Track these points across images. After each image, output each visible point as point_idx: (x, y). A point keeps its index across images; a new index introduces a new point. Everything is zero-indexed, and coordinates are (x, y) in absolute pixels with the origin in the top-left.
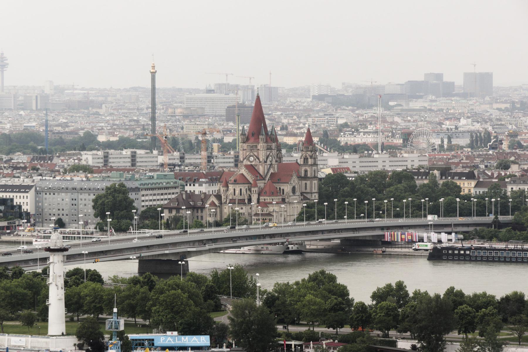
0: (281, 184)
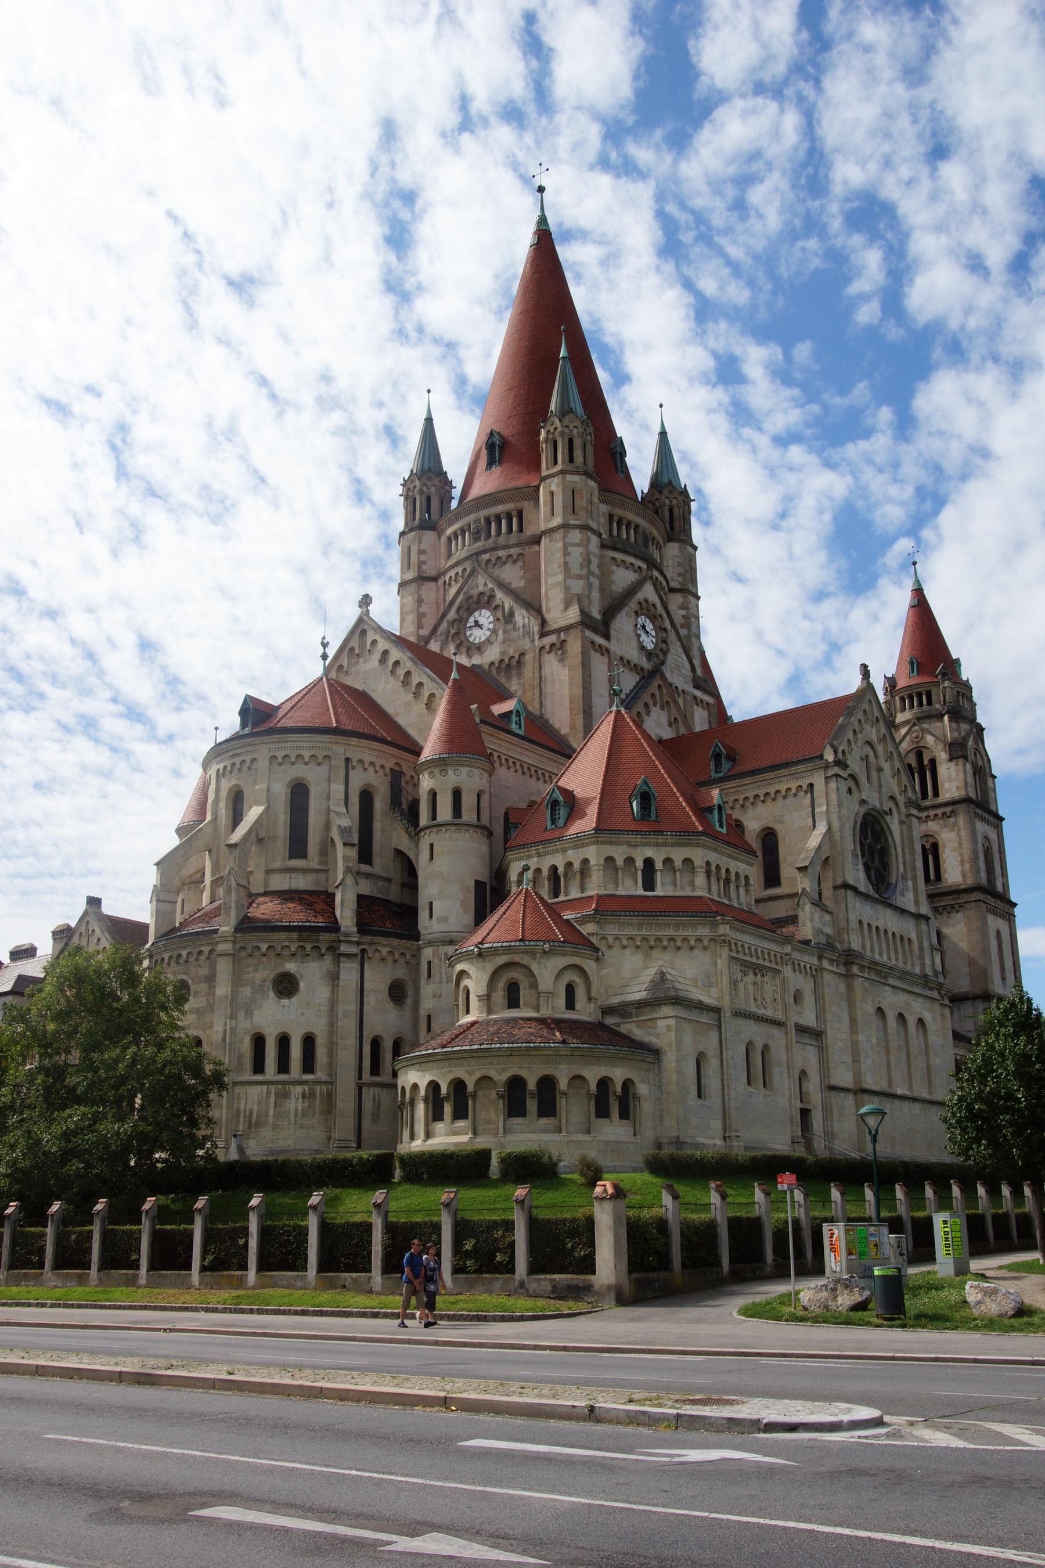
0: (750, 789)
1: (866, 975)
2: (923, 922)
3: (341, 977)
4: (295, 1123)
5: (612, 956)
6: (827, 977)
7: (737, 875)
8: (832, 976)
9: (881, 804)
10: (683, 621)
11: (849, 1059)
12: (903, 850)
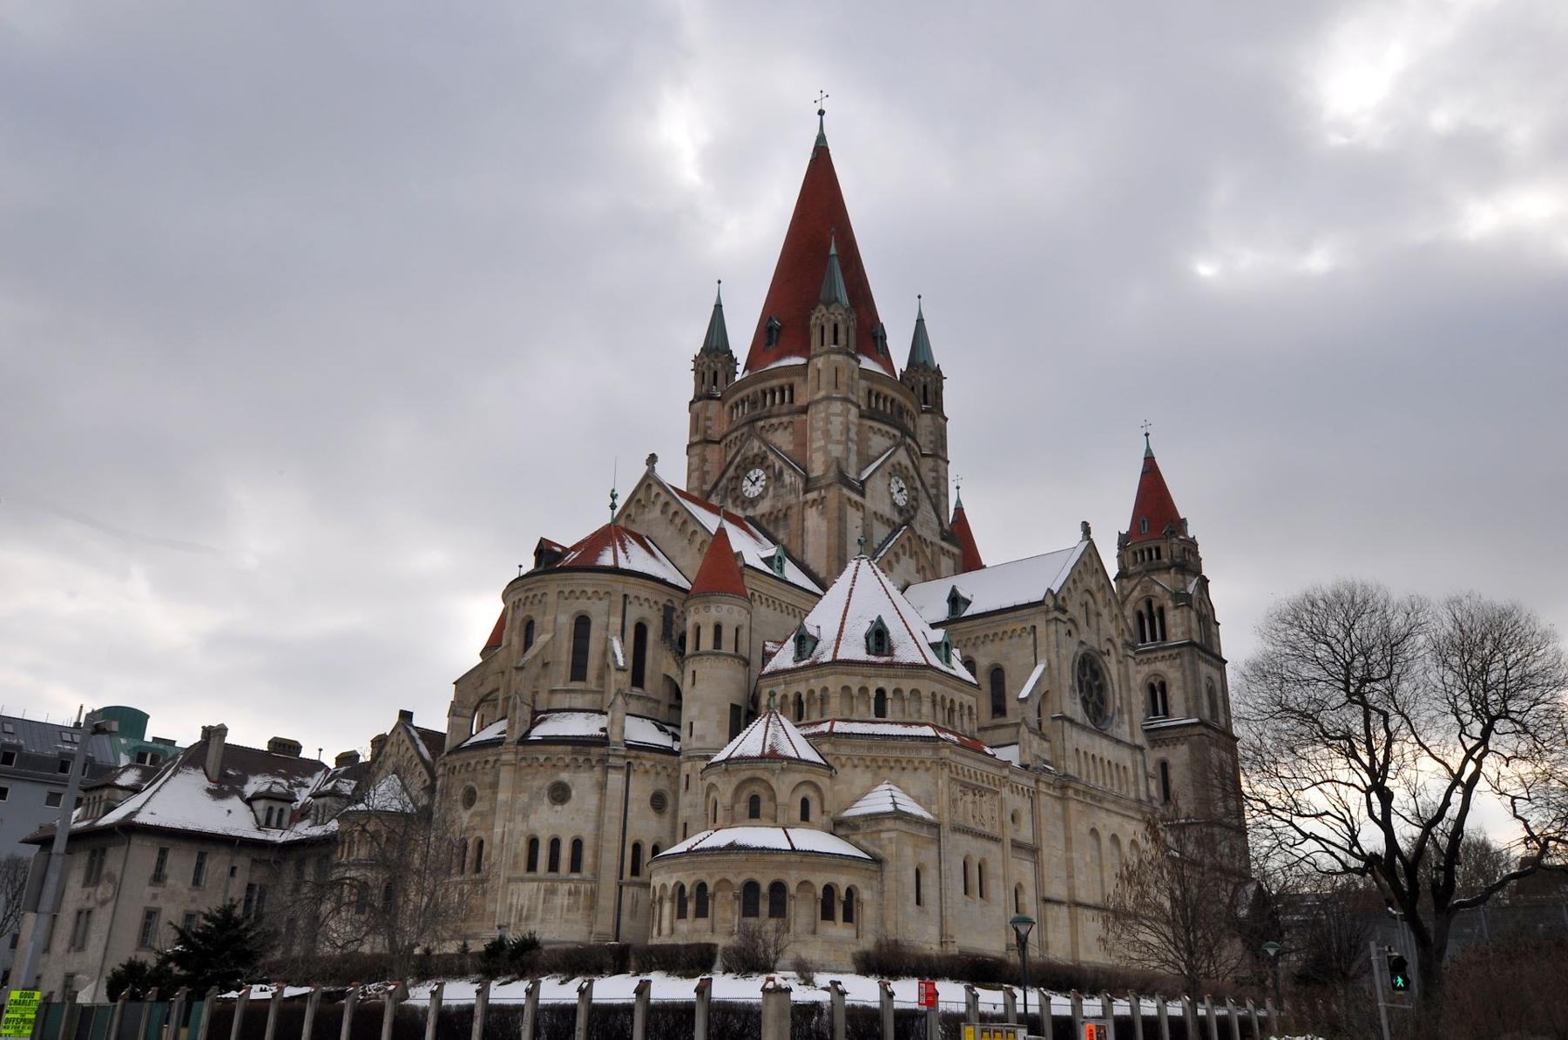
1: (1081, 798)
2: (1138, 752)
3: (608, 786)
4: (561, 918)
5: (844, 773)
6: (1043, 799)
7: (961, 705)
8: (1048, 798)
9: (1099, 644)
10: (933, 482)
11: (1063, 874)
12: (1120, 687)
